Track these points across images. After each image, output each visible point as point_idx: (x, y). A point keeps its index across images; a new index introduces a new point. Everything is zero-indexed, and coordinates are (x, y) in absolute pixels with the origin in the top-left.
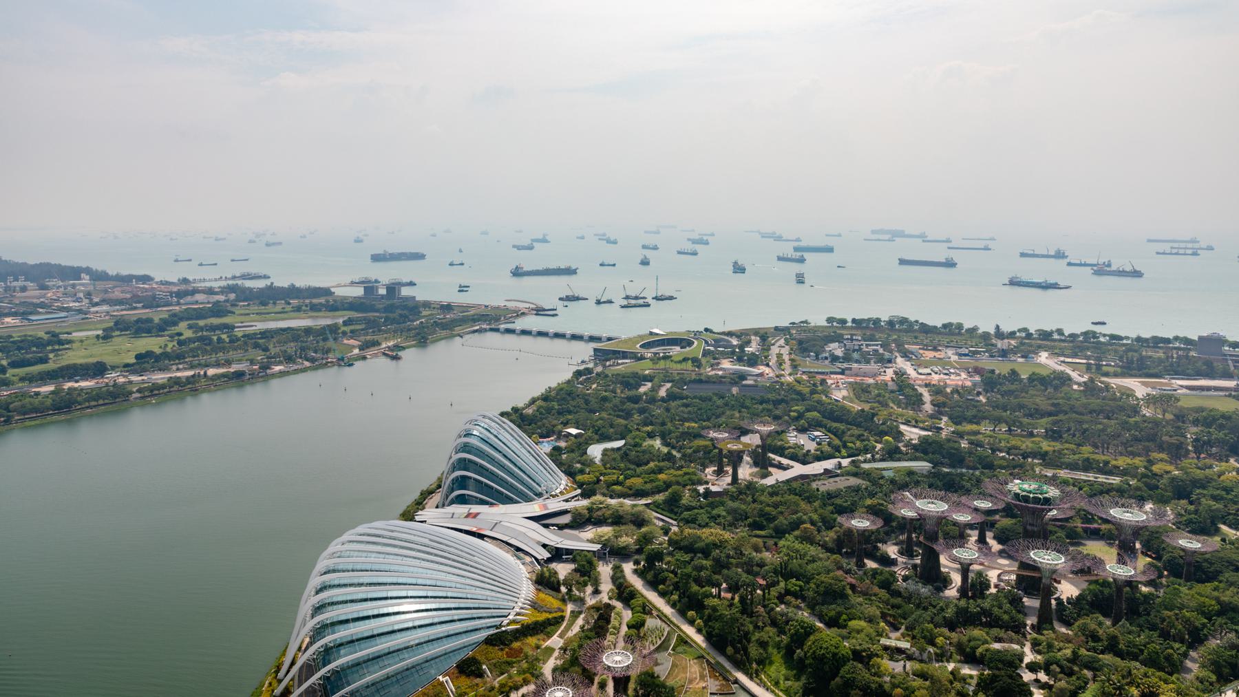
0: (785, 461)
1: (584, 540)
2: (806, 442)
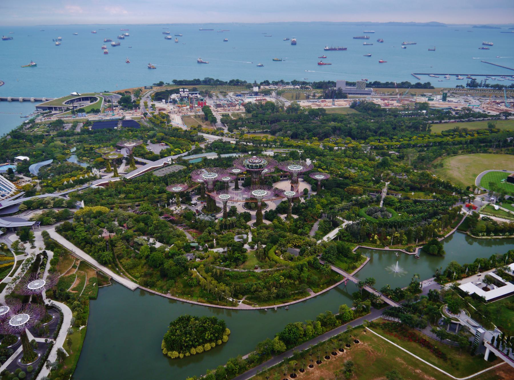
1: (26, 219)
2: (156, 149)
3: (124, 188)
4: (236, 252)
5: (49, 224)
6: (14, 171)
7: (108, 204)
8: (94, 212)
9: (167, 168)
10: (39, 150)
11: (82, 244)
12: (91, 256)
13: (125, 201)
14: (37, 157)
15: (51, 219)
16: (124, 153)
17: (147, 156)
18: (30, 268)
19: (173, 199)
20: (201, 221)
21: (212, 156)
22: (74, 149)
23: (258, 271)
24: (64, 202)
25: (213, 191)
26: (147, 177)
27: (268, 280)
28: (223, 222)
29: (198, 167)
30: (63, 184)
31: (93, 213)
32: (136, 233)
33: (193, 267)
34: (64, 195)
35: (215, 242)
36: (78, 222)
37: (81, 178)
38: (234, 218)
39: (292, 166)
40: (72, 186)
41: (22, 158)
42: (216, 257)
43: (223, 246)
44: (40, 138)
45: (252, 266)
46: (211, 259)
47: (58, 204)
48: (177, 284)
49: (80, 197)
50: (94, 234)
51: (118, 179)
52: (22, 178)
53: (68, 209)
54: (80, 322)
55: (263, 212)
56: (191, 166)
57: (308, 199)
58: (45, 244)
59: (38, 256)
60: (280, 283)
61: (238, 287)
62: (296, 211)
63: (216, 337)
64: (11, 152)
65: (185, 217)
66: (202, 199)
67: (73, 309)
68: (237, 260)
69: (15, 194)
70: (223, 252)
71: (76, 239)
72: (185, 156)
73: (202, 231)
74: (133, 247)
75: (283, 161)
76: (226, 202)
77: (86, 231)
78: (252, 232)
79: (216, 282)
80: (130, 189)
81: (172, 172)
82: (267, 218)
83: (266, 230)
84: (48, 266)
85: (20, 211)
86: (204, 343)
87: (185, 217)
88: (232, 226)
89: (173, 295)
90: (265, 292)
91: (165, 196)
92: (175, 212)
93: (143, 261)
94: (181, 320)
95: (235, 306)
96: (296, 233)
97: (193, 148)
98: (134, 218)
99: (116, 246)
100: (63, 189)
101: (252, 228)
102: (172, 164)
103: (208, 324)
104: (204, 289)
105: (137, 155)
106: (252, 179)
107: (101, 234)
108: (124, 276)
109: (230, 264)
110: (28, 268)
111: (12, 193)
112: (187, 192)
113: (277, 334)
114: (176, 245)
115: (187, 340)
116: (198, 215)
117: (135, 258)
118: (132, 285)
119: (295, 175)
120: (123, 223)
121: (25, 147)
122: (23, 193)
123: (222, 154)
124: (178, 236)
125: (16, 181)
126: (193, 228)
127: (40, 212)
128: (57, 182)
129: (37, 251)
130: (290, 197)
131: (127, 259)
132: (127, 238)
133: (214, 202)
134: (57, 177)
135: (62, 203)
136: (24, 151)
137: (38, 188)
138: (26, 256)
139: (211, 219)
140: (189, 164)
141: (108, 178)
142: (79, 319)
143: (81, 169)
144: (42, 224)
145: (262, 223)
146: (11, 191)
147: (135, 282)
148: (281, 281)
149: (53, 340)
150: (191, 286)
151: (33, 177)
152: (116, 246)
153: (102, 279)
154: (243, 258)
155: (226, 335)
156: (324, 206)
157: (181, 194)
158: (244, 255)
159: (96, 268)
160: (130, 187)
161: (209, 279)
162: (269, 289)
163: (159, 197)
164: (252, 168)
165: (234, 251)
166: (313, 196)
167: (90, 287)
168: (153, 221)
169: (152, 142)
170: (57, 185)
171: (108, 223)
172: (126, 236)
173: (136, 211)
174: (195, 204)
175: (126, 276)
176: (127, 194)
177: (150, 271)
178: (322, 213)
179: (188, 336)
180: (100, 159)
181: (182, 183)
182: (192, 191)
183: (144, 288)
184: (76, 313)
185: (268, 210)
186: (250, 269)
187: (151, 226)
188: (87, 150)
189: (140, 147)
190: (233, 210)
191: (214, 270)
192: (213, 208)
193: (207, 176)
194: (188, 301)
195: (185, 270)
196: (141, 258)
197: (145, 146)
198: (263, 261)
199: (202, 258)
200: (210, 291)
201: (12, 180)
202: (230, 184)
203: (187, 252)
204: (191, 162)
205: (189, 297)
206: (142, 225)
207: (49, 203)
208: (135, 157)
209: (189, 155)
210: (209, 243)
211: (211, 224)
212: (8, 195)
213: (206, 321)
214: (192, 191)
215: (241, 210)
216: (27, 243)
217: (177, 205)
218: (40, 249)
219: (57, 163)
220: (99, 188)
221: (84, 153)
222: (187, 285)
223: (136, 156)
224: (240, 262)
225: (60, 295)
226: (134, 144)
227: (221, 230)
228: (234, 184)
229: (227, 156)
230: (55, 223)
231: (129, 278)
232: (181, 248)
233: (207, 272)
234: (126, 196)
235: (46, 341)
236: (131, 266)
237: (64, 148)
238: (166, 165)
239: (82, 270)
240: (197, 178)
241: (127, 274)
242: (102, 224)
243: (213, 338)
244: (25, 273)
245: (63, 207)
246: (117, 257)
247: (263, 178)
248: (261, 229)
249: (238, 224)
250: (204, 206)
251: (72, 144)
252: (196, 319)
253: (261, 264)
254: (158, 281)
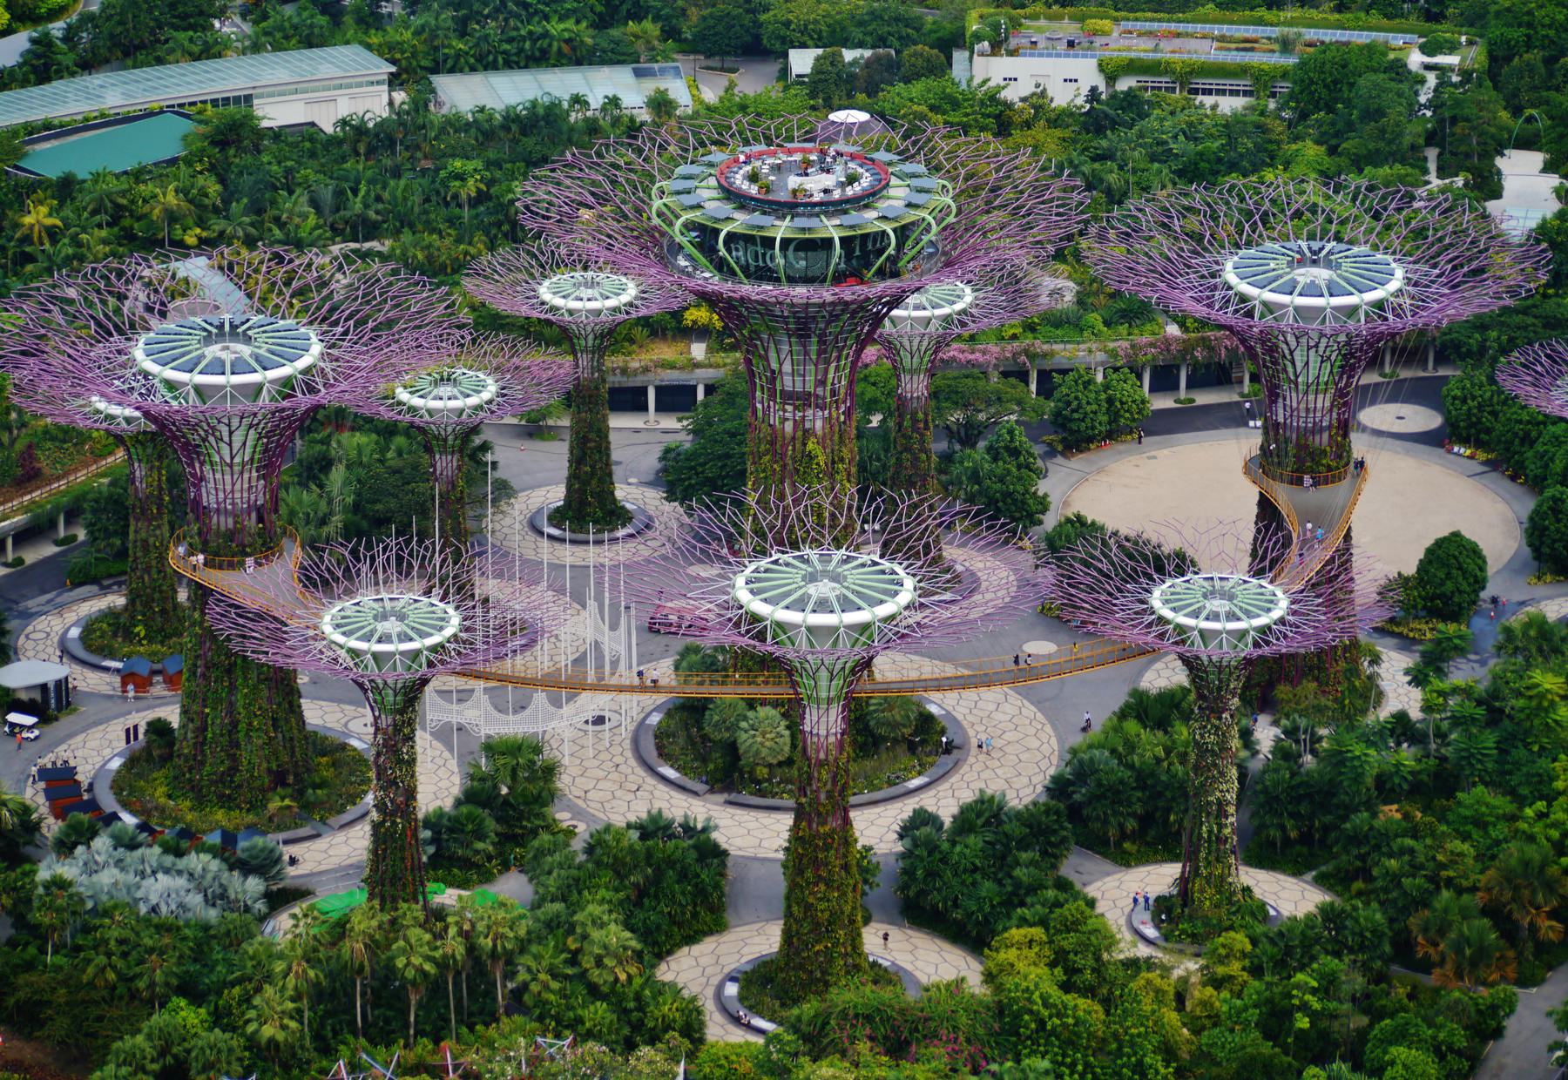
20: (86, 921)
25: (267, 547)
28: (354, 948)
38: (512, 888)
55: (877, 828)
56: (38, 216)
57: (1462, 674)
62: (1298, 822)
66: (150, 629)
75: (1191, 173)
76: (412, 693)
82: (921, 912)
101: (719, 1032)
106: (801, 408)
116: (65, 847)
119: (1310, 363)
123: (455, 67)
130: (1230, 654)
133: (283, 686)
145: (858, 964)
164: (764, 274)
174: (50, 704)
185: (945, 802)
190: (512, 799)
192: (254, 758)
202: (508, 457)
204: (47, 161)
215: (609, 787)
229: (508, 91)
240: (81, 385)
247: (916, 387)
249: (536, 971)
250: (159, 729)
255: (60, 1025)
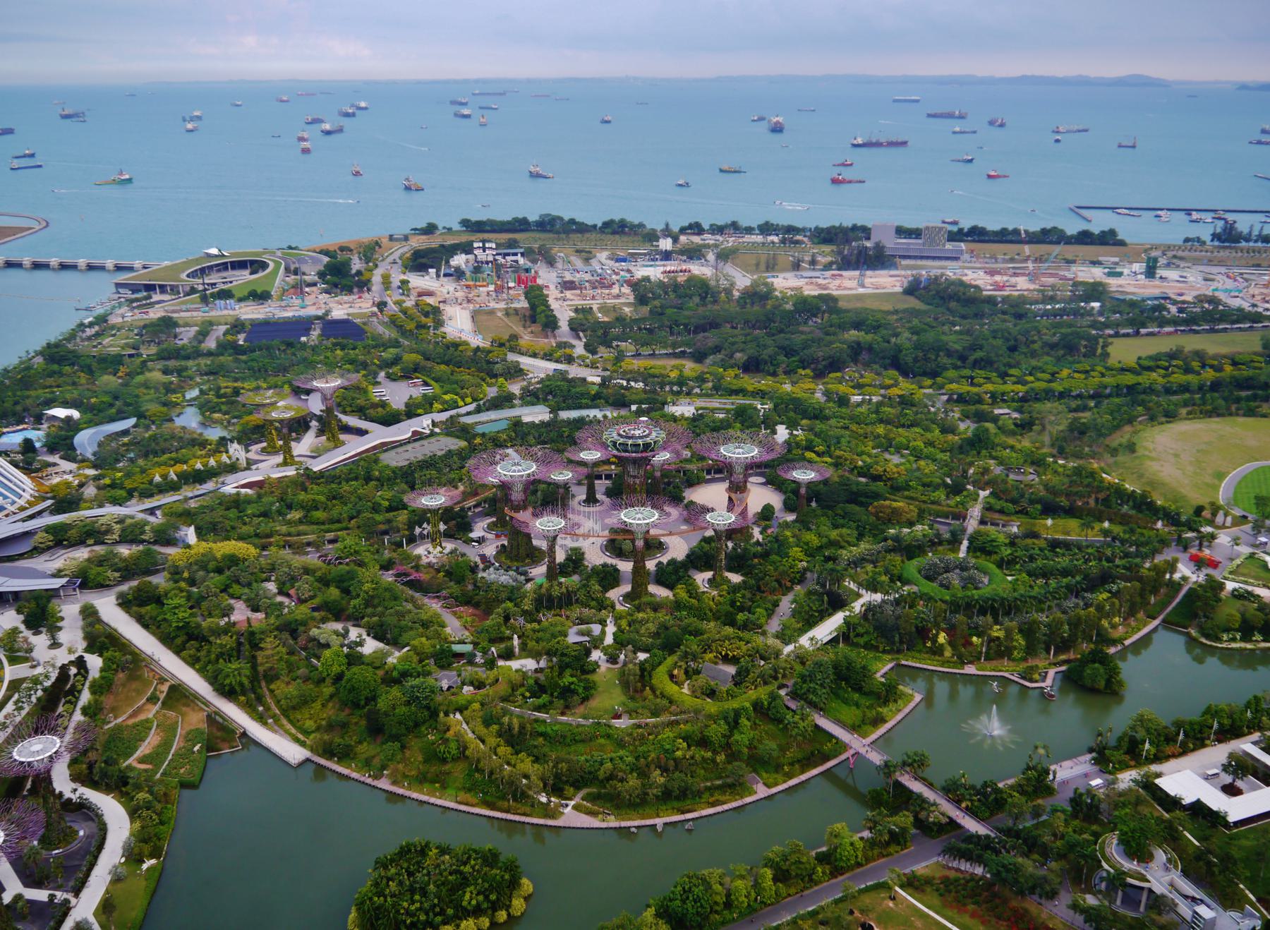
0: (364, 425)
2: (397, 394)
3: (302, 496)
4: (568, 672)
5: (102, 586)
6: (38, 445)
7: (257, 535)
8: (219, 555)
9: (417, 444)
10: (106, 393)
11: (179, 641)
12: (198, 671)
13: (301, 528)
14: (100, 411)
15: (109, 573)
16: (315, 405)
17: (371, 412)
18: (39, 699)
19: (425, 525)
20: (488, 586)
21: (536, 414)
22: (195, 393)
23: (623, 723)
24: (147, 528)
25: (525, 508)
26: (364, 469)
27: (644, 748)
28: (543, 591)
29: (497, 443)
30: (151, 482)
31: (215, 559)
32: (316, 614)
33: (452, 708)
34: (151, 511)
35: (516, 641)
36: (176, 582)
37: (199, 466)
38: (576, 578)
39: (731, 446)
40: (174, 487)
41: (61, 412)
42: (517, 684)
43: (536, 656)
44: (112, 363)
45: (606, 711)
46: (503, 688)
47: (131, 534)
48: (408, 753)
49: (187, 516)
50: (210, 615)
51: (290, 472)
52: (55, 465)
53: (157, 548)
54: (147, 849)
55: (651, 565)
56: (478, 441)
58: (85, 638)
59: (64, 669)
60: (675, 760)
61: (564, 765)
62: (737, 563)
63: (493, 903)
64: (38, 397)
65: (449, 574)
66: (502, 525)
67: (133, 813)
68: (567, 692)
69: (31, 504)
70: (536, 671)
71: (164, 625)
72: (468, 414)
73: (487, 613)
74: (305, 649)
75: (714, 430)
76: (555, 538)
77: (191, 608)
78: (617, 619)
79: (509, 749)
80: (317, 497)
81: (430, 454)
83: (652, 614)
84: (86, 697)
85: (37, 551)
86: (461, 919)
87: (449, 574)
88: (567, 600)
89: (394, 783)
90: (633, 781)
91: (402, 517)
92: (425, 561)
93: (328, 690)
94: (404, 852)
95: (553, 817)
96: (732, 623)
97: (492, 392)
98: (319, 574)
99: (261, 649)
100: (151, 496)
101: (618, 607)
102: (432, 434)
103: (473, 867)
104: (477, 770)
105: (348, 409)
107: (228, 615)
108: (276, 727)
109: (551, 702)
110: (34, 699)
111: (22, 502)
112: (462, 509)
113: (651, 901)
114: (414, 649)
115: (413, 908)
116: (484, 570)
117: (306, 679)
118: (293, 752)
119: (738, 469)
120: (288, 585)
121: (74, 384)
122: (49, 502)
124: (425, 625)
125: (38, 470)
126: (467, 603)
127: (82, 554)
128: (138, 478)
129: (62, 657)
130: (722, 528)
131: (288, 683)
132: (293, 626)
133: (528, 536)
134: (141, 462)
135: (143, 532)
136: (68, 396)
137: (90, 491)
138: (33, 667)
139: (515, 580)
140: (475, 436)
141: (270, 468)
142: (145, 841)
143: (203, 444)
144: (84, 586)
146: (20, 497)
147: (303, 744)
148: (679, 753)
149: (69, 896)
150: (444, 761)
151: (83, 461)
152: (261, 649)
153: (219, 734)
154: (585, 688)
155: (520, 896)
156: (810, 553)
157: (446, 514)
158: (587, 681)
159: (207, 703)
160: (316, 493)
161: (492, 741)
162: (643, 774)
163: (389, 521)
164: (626, 451)
165: (562, 668)
166: (786, 525)
167: (184, 755)
168: (363, 584)
169: (390, 377)
170: (135, 485)
171: (249, 585)
172: (290, 623)
173: (326, 556)
174: (481, 541)
175: (281, 726)
176: (308, 511)
177: (343, 716)
178: (805, 570)
179: (417, 897)
180: (256, 418)
181: (452, 484)
182: (475, 506)
183: (323, 762)
184: (138, 825)
185: (665, 559)
186: (600, 717)
187: (358, 596)
188: (224, 396)
189: (357, 388)
190: (575, 560)
191: (506, 719)
193: (514, 468)
194: (432, 800)
195: (430, 717)
196: (323, 680)
197: (370, 387)
198: (637, 696)
199: (479, 685)
200: (491, 773)
201: (27, 468)
202: (574, 489)
203: (442, 667)
204: (480, 429)
205: (435, 790)
206: (334, 593)
207: (109, 531)
208: (341, 416)
209: (478, 410)
210: (503, 646)
211: (513, 594)
212: (12, 508)
213: (469, 858)
214: (475, 506)
215: (595, 557)
216: (40, 633)
217: (433, 540)
218: (70, 651)
219: (147, 428)
220: (238, 494)
221: (218, 404)
222: (433, 756)
223: (344, 412)
224: (576, 698)
225: (104, 775)
226: (338, 382)
227: (538, 611)
228: (584, 489)
230: (119, 583)
231: (287, 732)
232: (428, 658)
233: (487, 723)
234: (305, 517)
235: (52, 897)
236: (295, 701)
237: (169, 389)
238: (417, 437)
239: (170, 709)
240: (487, 475)
241: (285, 722)
242: (236, 589)
243: (485, 905)
244: (24, 713)
245: (143, 541)
246: (265, 676)
247: (658, 474)
248: (639, 609)
249: (581, 595)
250: (503, 546)
251: (191, 379)
252: (443, 851)
253: (632, 705)
254: (360, 742)
255: (483, 607)
